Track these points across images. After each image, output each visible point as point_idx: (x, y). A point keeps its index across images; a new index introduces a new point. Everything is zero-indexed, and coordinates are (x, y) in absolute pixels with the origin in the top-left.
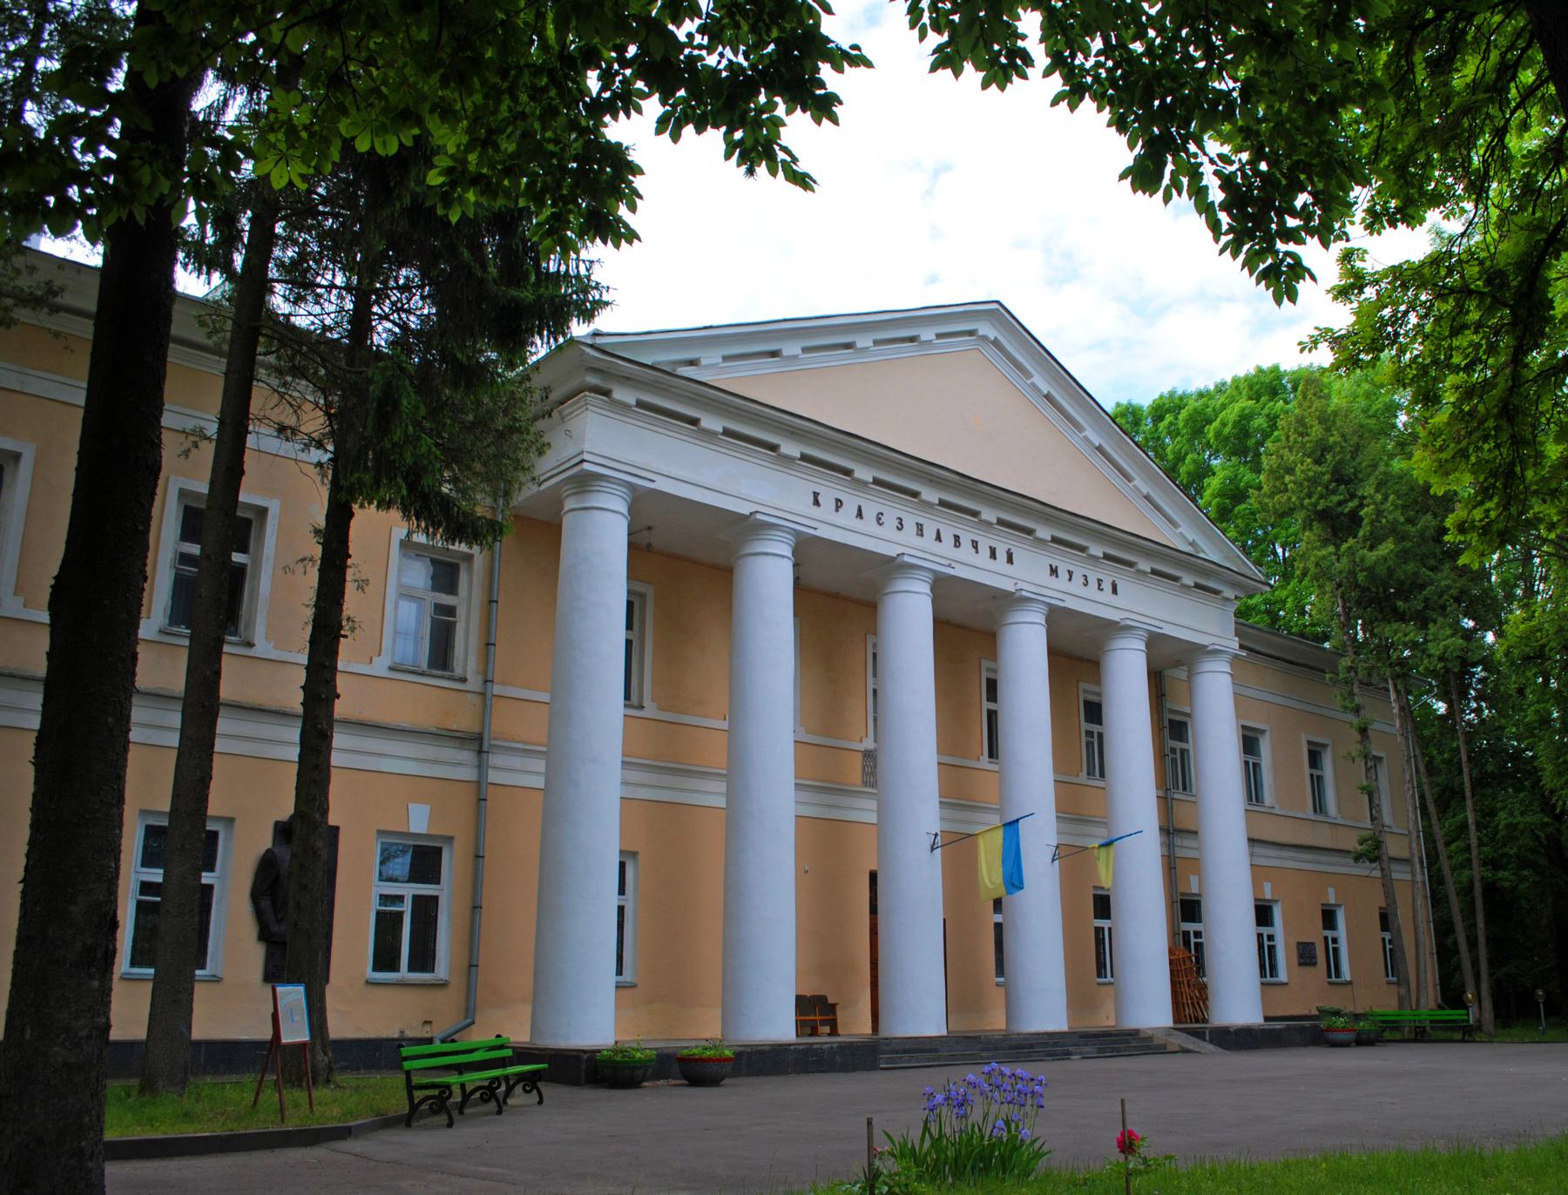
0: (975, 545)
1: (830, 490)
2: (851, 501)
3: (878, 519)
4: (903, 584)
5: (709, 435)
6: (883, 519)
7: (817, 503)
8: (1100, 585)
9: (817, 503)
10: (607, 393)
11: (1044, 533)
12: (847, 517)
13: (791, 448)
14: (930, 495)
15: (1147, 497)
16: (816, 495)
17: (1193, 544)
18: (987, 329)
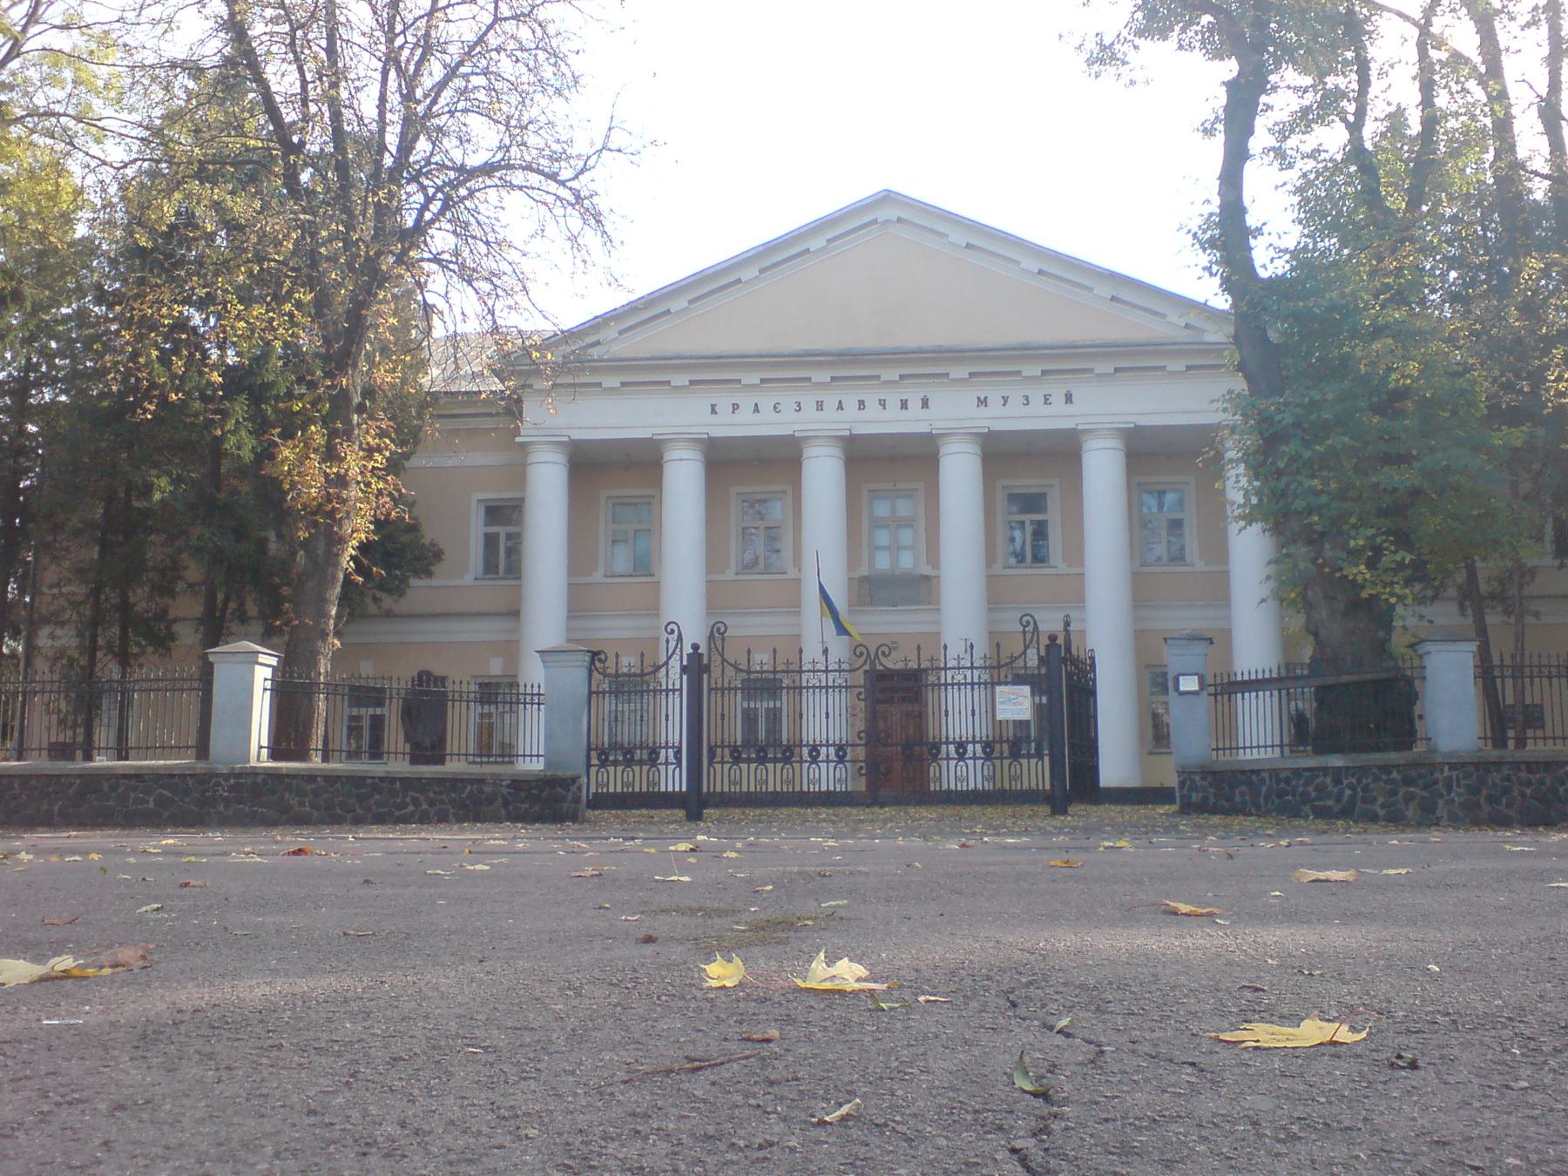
0: (883, 403)
1: (724, 401)
2: (747, 403)
3: (775, 408)
4: (809, 452)
5: (611, 391)
6: (779, 407)
7: (714, 411)
8: (1046, 400)
9: (714, 411)
10: (531, 386)
11: (959, 372)
12: (745, 414)
13: (680, 380)
14: (822, 376)
15: (1113, 299)
16: (713, 407)
17: (1187, 326)
18: (890, 213)
